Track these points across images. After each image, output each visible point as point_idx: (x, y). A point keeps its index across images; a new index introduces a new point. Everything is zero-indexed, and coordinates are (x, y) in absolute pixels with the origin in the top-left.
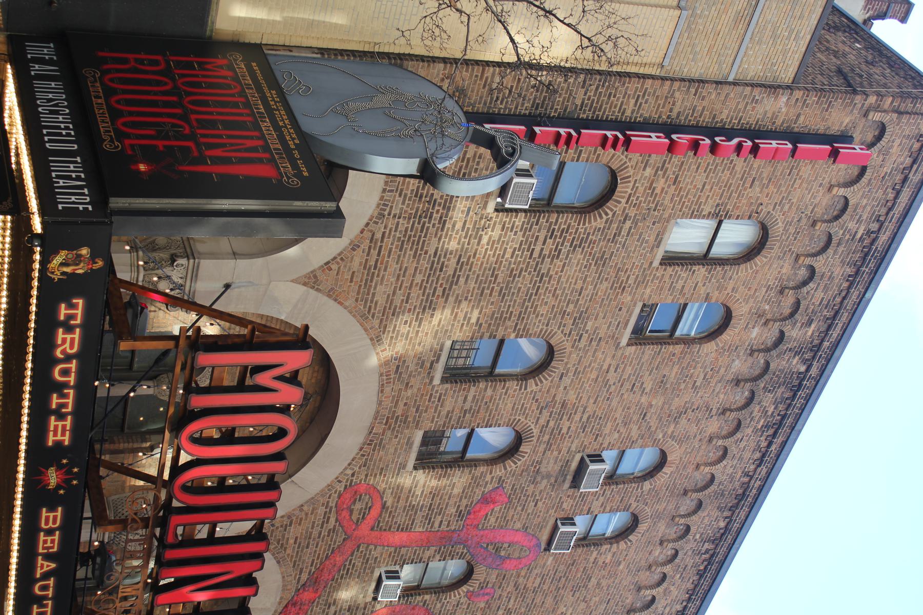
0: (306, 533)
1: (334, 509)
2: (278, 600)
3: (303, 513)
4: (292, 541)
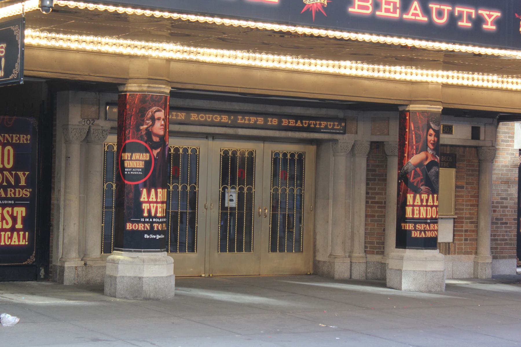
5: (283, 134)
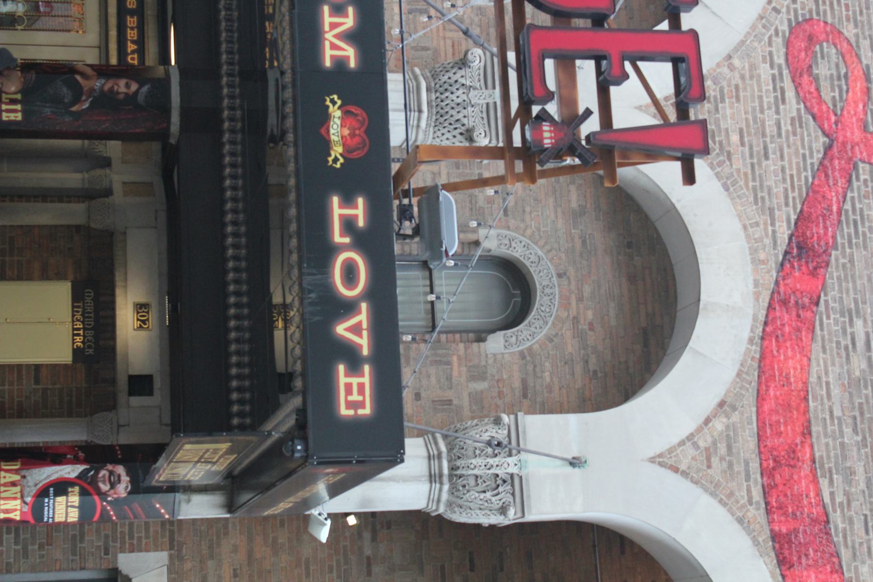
0: (755, 121)
1: (785, 72)
2: (751, 286)
3: (737, 75)
4: (735, 138)
5: (113, 21)
